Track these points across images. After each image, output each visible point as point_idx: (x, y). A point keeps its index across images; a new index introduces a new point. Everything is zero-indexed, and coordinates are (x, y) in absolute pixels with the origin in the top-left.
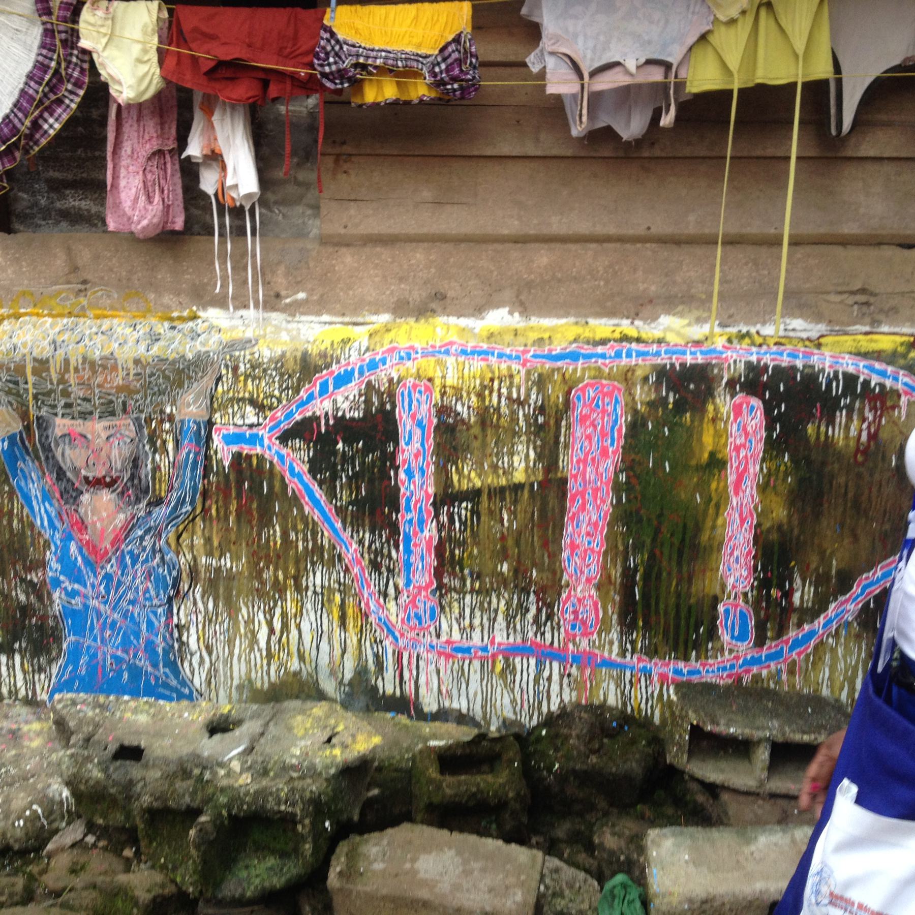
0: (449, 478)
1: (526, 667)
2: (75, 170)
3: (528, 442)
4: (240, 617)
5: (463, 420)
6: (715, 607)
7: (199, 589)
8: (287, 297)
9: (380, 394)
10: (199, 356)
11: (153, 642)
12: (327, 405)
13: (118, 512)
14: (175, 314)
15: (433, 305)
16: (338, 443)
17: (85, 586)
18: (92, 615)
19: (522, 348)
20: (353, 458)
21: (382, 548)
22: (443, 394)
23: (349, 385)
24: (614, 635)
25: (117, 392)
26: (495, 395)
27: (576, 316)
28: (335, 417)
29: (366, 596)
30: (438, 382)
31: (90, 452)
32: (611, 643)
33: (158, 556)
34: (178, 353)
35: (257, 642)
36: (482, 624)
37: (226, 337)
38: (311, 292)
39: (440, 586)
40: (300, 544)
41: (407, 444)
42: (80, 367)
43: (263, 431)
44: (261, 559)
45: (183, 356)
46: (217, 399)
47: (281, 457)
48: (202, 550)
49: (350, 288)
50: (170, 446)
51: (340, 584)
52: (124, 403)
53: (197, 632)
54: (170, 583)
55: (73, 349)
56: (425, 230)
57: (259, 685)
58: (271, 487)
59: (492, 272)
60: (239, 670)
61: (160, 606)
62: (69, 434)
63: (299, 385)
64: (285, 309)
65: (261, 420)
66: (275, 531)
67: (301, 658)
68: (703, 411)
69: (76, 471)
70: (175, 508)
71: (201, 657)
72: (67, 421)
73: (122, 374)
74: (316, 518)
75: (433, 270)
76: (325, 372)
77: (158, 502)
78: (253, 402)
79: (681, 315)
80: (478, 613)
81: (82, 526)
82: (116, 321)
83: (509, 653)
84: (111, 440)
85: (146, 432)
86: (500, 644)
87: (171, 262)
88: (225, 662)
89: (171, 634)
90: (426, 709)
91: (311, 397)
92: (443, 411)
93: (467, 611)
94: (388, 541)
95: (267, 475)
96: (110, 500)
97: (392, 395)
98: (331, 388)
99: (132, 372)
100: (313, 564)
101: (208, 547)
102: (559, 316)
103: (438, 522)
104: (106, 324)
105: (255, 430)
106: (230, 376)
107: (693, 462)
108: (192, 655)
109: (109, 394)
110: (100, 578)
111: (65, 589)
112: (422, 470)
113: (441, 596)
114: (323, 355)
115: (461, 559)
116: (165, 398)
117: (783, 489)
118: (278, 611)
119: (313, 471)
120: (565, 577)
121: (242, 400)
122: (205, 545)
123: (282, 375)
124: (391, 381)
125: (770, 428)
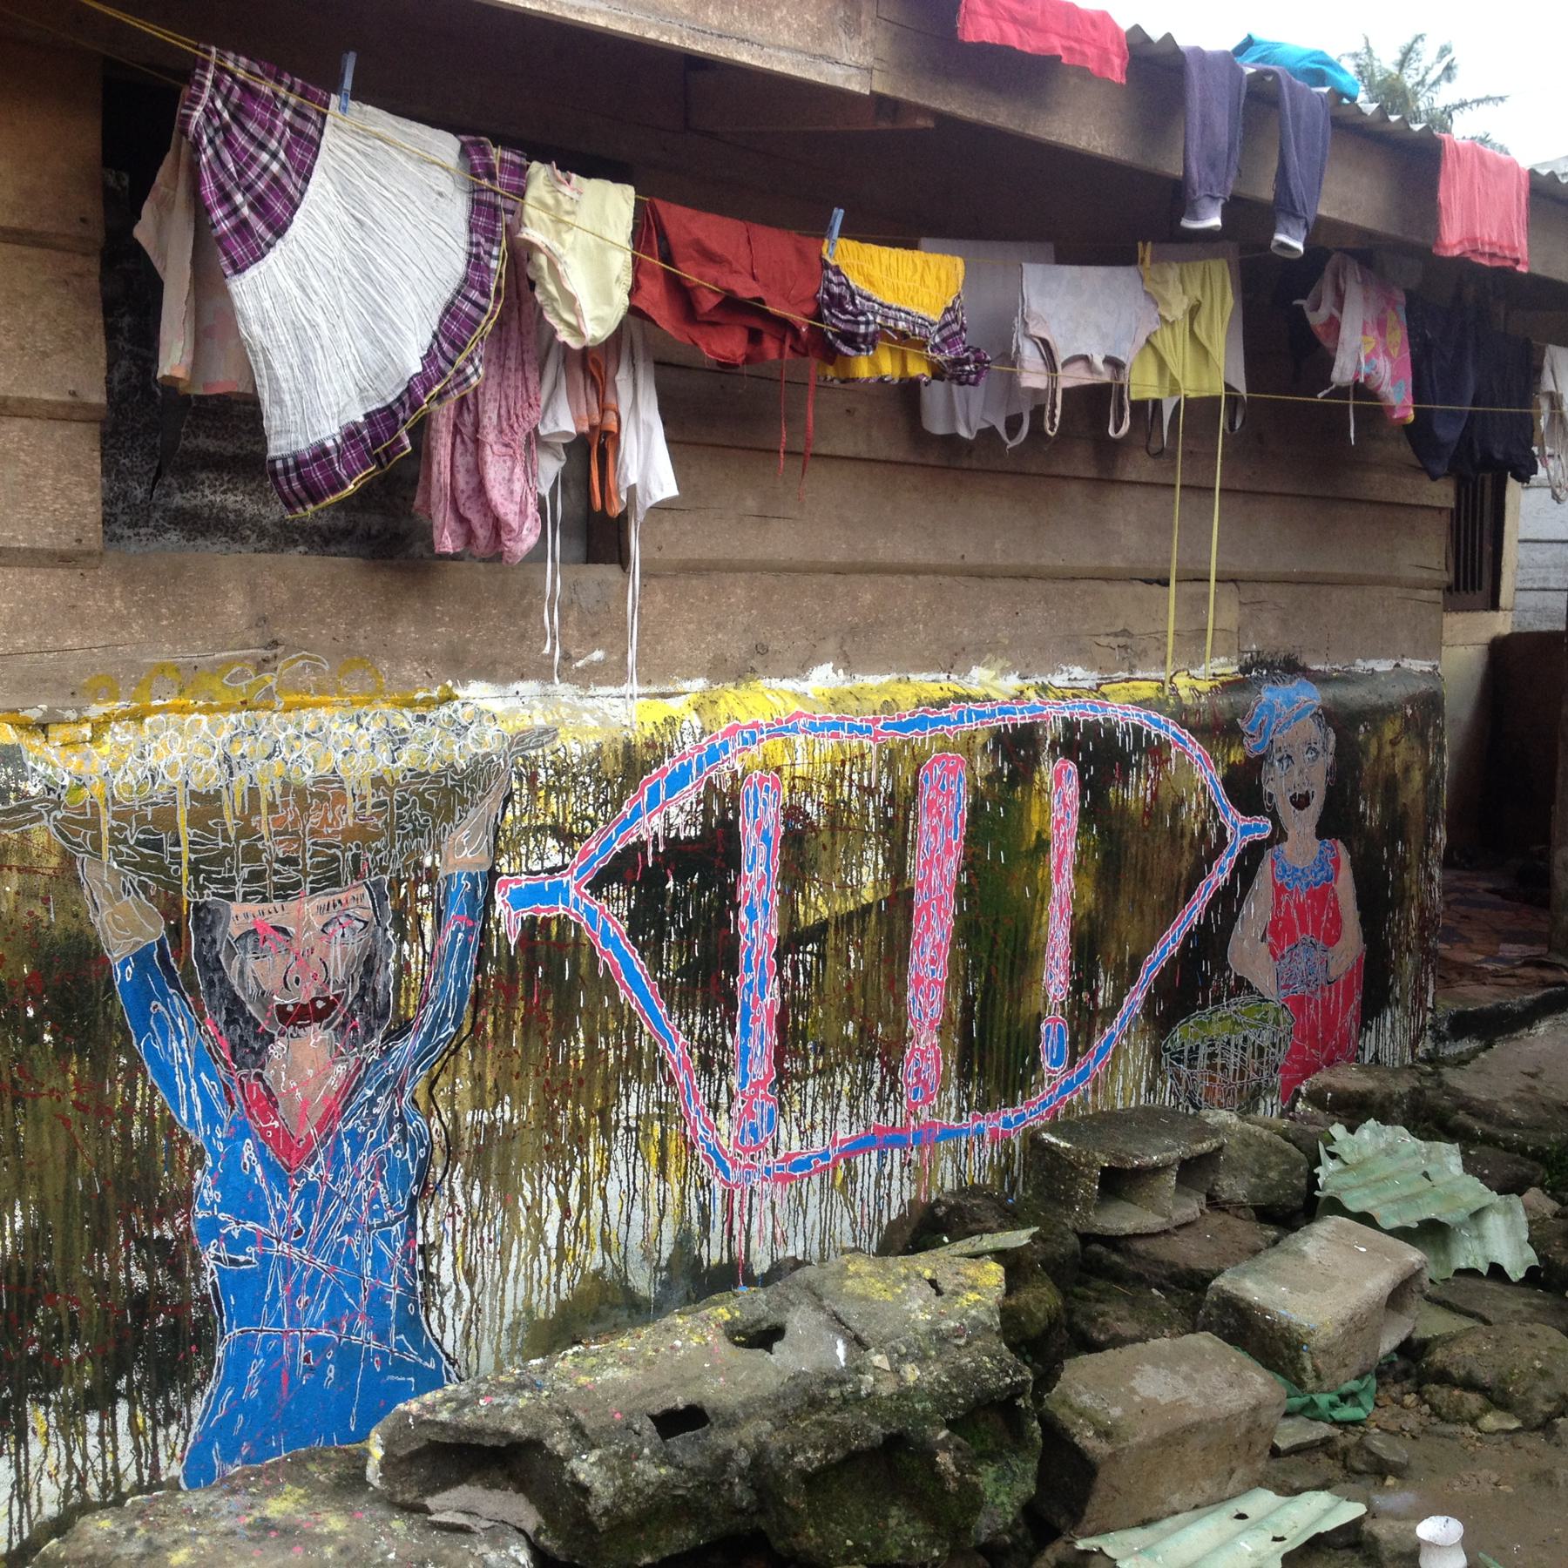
0: (795, 912)
1: (867, 1164)
2: (244, 438)
4: (521, 1203)
6: (1038, 1029)
7: (459, 1170)
9: (721, 797)
10: (477, 762)
11: (382, 1291)
13: (334, 1062)
14: (420, 695)
15: (753, 663)
17: (265, 1220)
18: (275, 1271)
20: (686, 901)
21: (715, 1034)
22: (792, 789)
24: (953, 1093)
25: (344, 841)
26: (846, 783)
28: (666, 839)
29: (693, 1115)
30: (786, 772)
31: (292, 958)
32: (950, 1103)
33: (396, 1127)
35: (543, 1240)
36: (823, 1121)
37: (509, 728)
38: (609, 651)
39: (782, 1073)
40: (611, 1053)
42: (278, 801)
44: (555, 1092)
45: (452, 765)
46: (504, 832)
47: (591, 914)
48: (468, 1102)
49: (658, 642)
50: (428, 925)
51: (660, 1104)
52: (356, 858)
53: (454, 1251)
54: (414, 1172)
55: (262, 770)
57: (542, 1316)
60: (514, 1294)
61: (397, 1219)
66: (577, 1040)
67: (606, 1245)
68: (1032, 781)
69: (263, 998)
70: (429, 1035)
71: (458, 1292)
72: (253, 907)
73: (352, 806)
76: (655, 771)
77: (402, 1028)
78: (558, 832)
79: (988, 666)
81: (269, 1102)
82: (322, 712)
83: (852, 1150)
84: (330, 929)
85: (389, 905)
86: (842, 1141)
88: (493, 1294)
89: (412, 1266)
90: (757, 1272)
91: (637, 813)
92: (792, 813)
93: (809, 1103)
96: (323, 1041)
97: (735, 798)
98: (662, 796)
99: (371, 801)
100: (627, 1081)
102: (882, 673)
104: (309, 720)
105: (558, 877)
106: (525, 792)
107: (1023, 849)
108: (443, 1294)
110: (294, 1196)
111: (229, 1236)
112: (765, 903)
113: (781, 1091)
114: (651, 745)
115: (805, 1027)
117: (1092, 869)
118: (577, 1174)
119: (632, 933)
120: (910, 1025)
123: (598, 781)
124: (734, 776)
125: (1082, 797)
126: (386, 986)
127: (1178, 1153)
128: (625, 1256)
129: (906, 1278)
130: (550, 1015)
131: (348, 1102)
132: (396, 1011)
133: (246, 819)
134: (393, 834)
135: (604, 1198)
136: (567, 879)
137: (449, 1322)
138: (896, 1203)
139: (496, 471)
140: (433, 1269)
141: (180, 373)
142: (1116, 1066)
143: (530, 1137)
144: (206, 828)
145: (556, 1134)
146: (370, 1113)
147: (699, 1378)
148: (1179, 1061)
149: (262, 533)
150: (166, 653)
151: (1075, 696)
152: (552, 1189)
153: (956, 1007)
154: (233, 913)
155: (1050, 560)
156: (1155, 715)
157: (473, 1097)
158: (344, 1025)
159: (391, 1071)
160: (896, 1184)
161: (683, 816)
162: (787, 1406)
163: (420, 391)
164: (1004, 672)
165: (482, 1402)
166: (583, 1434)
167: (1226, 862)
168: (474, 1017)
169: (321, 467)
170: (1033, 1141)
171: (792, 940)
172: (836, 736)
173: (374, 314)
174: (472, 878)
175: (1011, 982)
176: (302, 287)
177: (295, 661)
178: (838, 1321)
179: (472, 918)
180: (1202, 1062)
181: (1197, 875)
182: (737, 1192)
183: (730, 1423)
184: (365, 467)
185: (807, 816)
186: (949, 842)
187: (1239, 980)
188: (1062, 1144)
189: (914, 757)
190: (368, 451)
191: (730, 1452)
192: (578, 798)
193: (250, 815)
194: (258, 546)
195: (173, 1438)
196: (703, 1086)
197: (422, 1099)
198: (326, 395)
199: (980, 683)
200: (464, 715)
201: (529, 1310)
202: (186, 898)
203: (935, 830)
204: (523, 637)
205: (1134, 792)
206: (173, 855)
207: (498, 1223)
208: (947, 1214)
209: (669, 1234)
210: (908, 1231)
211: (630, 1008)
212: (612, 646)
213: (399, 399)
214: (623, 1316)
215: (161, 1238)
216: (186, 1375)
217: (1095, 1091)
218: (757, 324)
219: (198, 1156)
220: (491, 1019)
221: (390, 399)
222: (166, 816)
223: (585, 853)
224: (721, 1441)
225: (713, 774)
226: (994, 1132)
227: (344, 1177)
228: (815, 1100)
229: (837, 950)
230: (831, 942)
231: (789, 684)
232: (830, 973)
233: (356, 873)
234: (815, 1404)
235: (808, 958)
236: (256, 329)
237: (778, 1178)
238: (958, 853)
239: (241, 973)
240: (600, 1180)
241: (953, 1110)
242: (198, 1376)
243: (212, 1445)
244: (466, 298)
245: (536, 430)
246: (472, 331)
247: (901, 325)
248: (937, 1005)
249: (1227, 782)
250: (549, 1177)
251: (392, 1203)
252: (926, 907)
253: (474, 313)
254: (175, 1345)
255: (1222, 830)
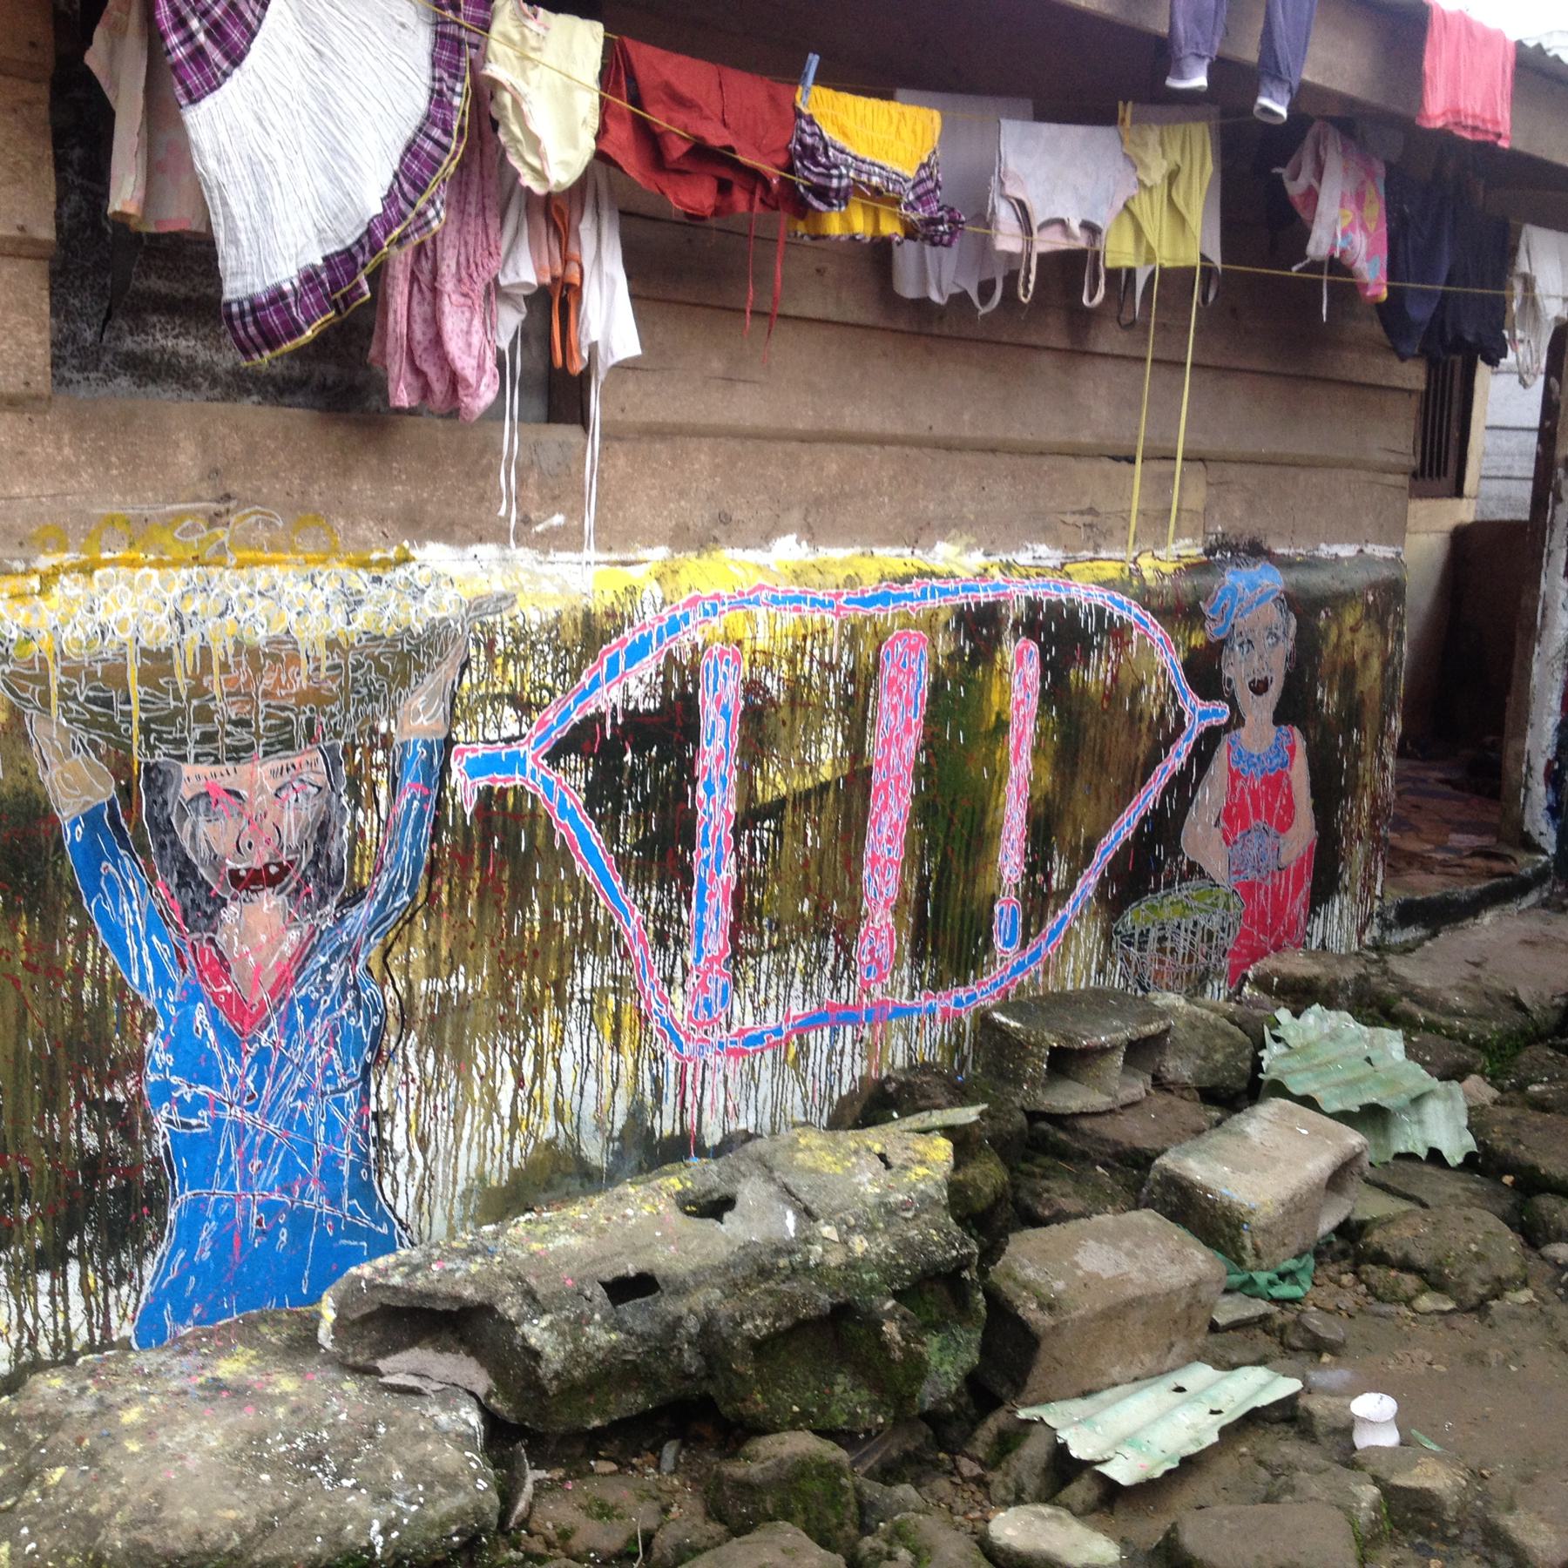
0: (753, 787)
1: (819, 1040)
2: (197, 280)
3: (838, 719)
5: (771, 699)
8: (538, 523)
9: (681, 669)
12: (616, 695)
13: (288, 928)
14: (376, 556)
15: (716, 533)
16: (625, 753)
17: (218, 1084)
18: (228, 1135)
19: (834, 591)
20: (643, 774)
22: (752, 663)
23: (645, 660)
24: (905, 972)
26: (807, 658)
27: (862, 545)
28: (625, 712)
29: (647, 988)
30: (747, 645)
31: (244, 821)
32: (903, 982)
33: (350, 995)
34: (399, 626)
37: (467, 594)
38: (569, 517)
40: (567, 925)
41: (709, 743)
43: (526, 748)
44: (510, 963)
45: (409, 629)
46: (461, 700)
47: (548, 786)
48: (422, 971)
49: (620, 508)
50: (382, 792)
51: (614, 978)
52: (310, 722)
53: (407, 1119)
54: (367, 1040)
55: (215, 629)
56: (715, 419)
57: (494, 1183)
58: (531, 838)
59: (781, 483)
60: (467, 1162)
61: (351, 1085)
62: (207, 794)
63: (580, 664)
64: (531, 544)
65: (524, 729)
66: (532, 912)
67: (559, 1114)
68: (993, 661)
69: (216, 862)
70: (384, 903)
71: (411, 1158)
72: (205, 769)
73: (306, 668)
74: (589, 879)
75: (718, 479)
76: (614, 641)
77: (356, 896)
78: (515, 700)
79: (953, 541)
80: (774, 979)
81: (221, 966)
82: (276, 571)
84: (283, 794)
85: (344, 770)
86: (795, 1018)
87: (374, 462)
88: (446, 1161)
89: (365, 1133)
90: (708, 1144)
91: (595, 684)
92: (752, 687)
93: (763, 978)
94: (678, 899)
95: (527, 820)
96: (276, 907)
97: (695, 670)
99: (325, 664)
100: (582, 954)
101: (432, 961)
103: (738, 853)
104: (262, 577)
105: (515, 747)
106: (482, 658)
107: (983, 729)
108: (396, 1160)
109: (283, 709)
110: (247, 1061)
111: (181, 1100)
112: (723, 780)
113: (736, 967)
114: (611, 615)
115: (761, 904)
116: (379, 707)
117: (1050, 751)
118: (531, 1045)
119: (589, 805)
120: (865, 904)
121: (498, 697)
122: (428, 958)
123: (556, 650)
124: (694, 648)
125: (1043, 678)
126: (340, 853)
127: (1127, 1033)
128: (578, 1127)
129: (856, 1152)
130: (506, 889)
131: (302, 968)
132: (350, 879)
133: (199, 680)
134: (347, 698)
135: (558, 1069)
136: (525, 749)
137: (402, 1189)
138: (847, 1078)
139: (454, 323)
140: (386, 1136)
141: (132, 209)
142: (1067, 948)
143: (485, 1008)
144: (158, 687)
145: (510, 1005)
146: (324, 980)
147: (650, 1245)
148: (1130, 944)
149: (215, 382)
150: (115, 504)
151: (1038, 575)
152: (506, 1060)
153: (911, 888)
154: (185, 775)
155: (1018, 433)
156: (1118, 597)
157: (428, 966)
158: (297, 891)
159: (345, 939)
160: (847, 1060)
161: (642, 687)
162: (738, 1274)
163: (380, 233)
164: (969, 548)
165: (434, 1267)
166: (534, 1299)
167: (1183, 746)
168: (429, 887)
169: (278, 311)
170: (984, 1020)
171: (749, 816)
172: (798, 609)
173: (334, 151)
174: (426, 744)
175: (967, 863)
176: (260, 121)
177: (246, 516)
178: (788, 1192)
179: (428, 785)
180: (1152, 945)
181: (1153, 760)
182: (690, 1066)
183: (681, 1290)
184: (324, 312)
185: (767, 691)
186: (908, 722)
187: (1192, 865)
188: (1013, 1024)
189: (876, 633)
190: (327, 296)
191: (680, 1318)
192: (536, 666)
193: (202, 673)
194: (210, 394)
195: (124, 1298)
196: (658, 960)
197: (376, 967)
198: (283, 235)
199: (945, 560)
200: (421, 578)
201: (482, 1178)
202: (136, 758)
203: (895, 708)
204: (482, 498)
205: (1095, 675)
206: (123, 713)
207: (452, 1091)
208: (897, 1090)
209: (622, 1104)
210: (858, 1106)
211: (586, 882)
212: (573, 510)
213: (359, 242)
214: (575, 1184)
215: (113, 1101)
216: (138, 1236)
217: (1046, 972)
218: (727, 174)
219: (150, 1020)
220: (446, 888)
221: (349, 242)
222: (115, 674)
223: (542, 723)
224: (671, 1308)
225: (673, 646)
226: (945, 1011)
227: (297, 1043)
228: (769, 976)
229: (794, 827)
230: (789, 819)
231: (754, 556)
232: (787, 851)
233: (310, 737)
234: (764, 1273)
235: (766, 834)
236: (211, 164)
237: (730, 1053)
238: (918, 732)
239: (193, 836)
240: (554, 1050)
241: (906, 989)
242: (150, 1237)
243: (163, 1306)
244: (428, 136)
245: (496, 280)
246: (434, 171)
247: (875, 180)
248: (893, 885)
249: (1187, 666)
250: (503, 1047)
251: (345, 1069)
252: (884, 786)
253: (436, 152)
254: (127, 1207)
255: (1180, 714)
